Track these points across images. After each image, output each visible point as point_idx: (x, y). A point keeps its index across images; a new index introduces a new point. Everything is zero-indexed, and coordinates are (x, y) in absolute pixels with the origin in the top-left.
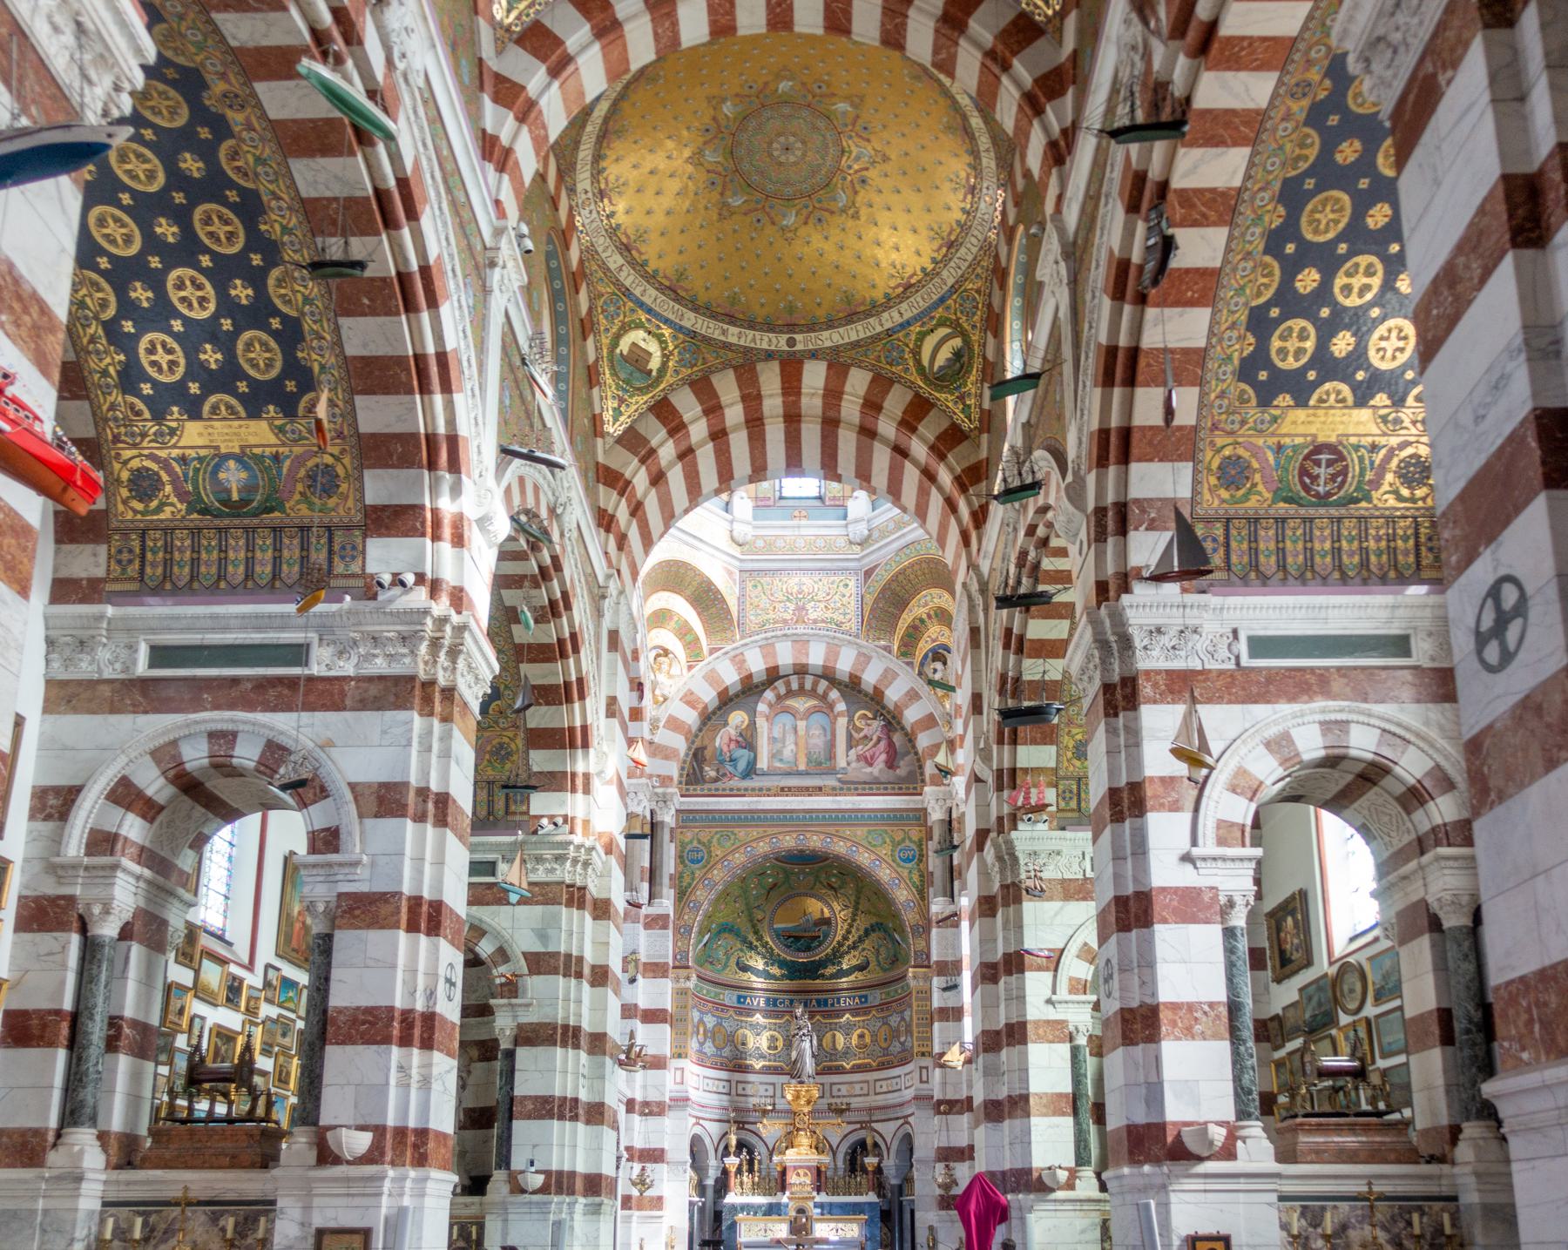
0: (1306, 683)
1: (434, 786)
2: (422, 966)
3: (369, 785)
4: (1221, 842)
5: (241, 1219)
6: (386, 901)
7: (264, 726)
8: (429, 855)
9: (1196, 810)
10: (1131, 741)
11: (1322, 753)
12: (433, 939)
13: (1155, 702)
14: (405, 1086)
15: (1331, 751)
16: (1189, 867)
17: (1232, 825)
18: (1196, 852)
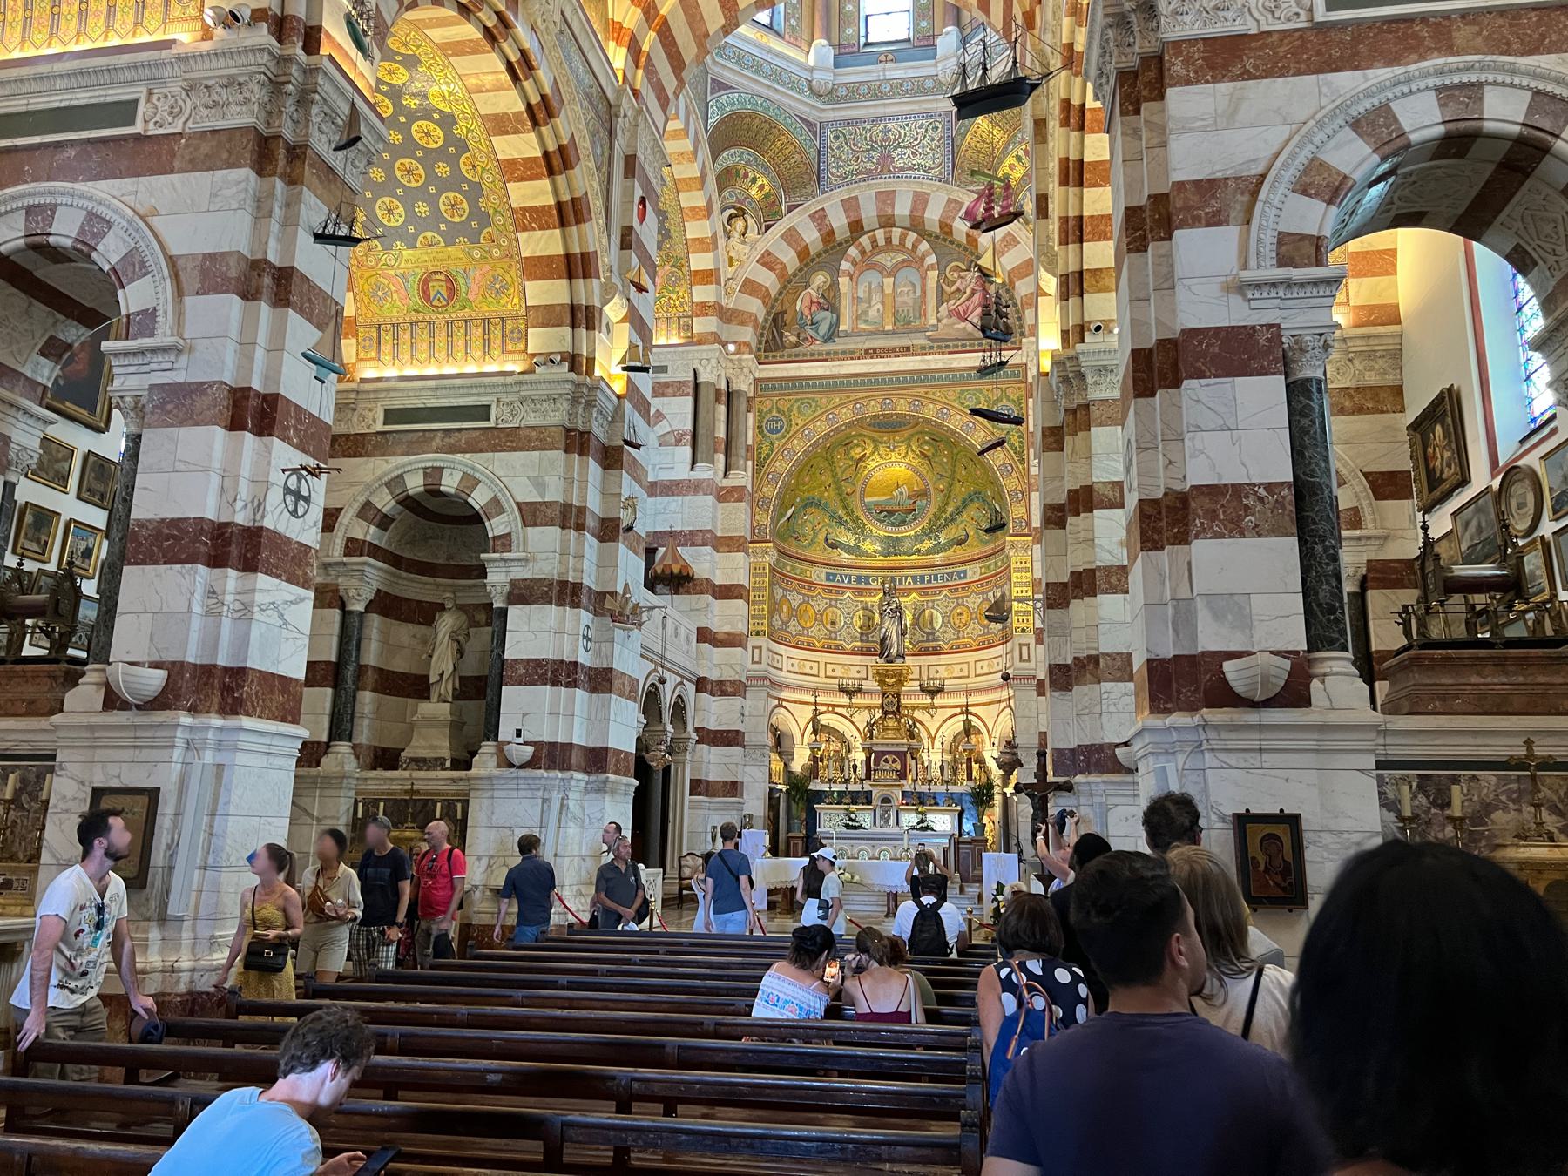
0: (1415, 36)
1: (273, 257)
2: (246, 471)
3: (193, 257)
4: (1282, 263)
5: (32, 777)
6: (204, 392)
7: (81, 196)
8: (262, 339)
9: (1248, 223)
10: (1156, 141)
11: (1441, 130)
12: (266, 439)
13: (1188, 83)
14: (213, 614)
15: (1452, 126)
16: (1236, 300)
17: (1303, 237)
18: (1247, 275)
